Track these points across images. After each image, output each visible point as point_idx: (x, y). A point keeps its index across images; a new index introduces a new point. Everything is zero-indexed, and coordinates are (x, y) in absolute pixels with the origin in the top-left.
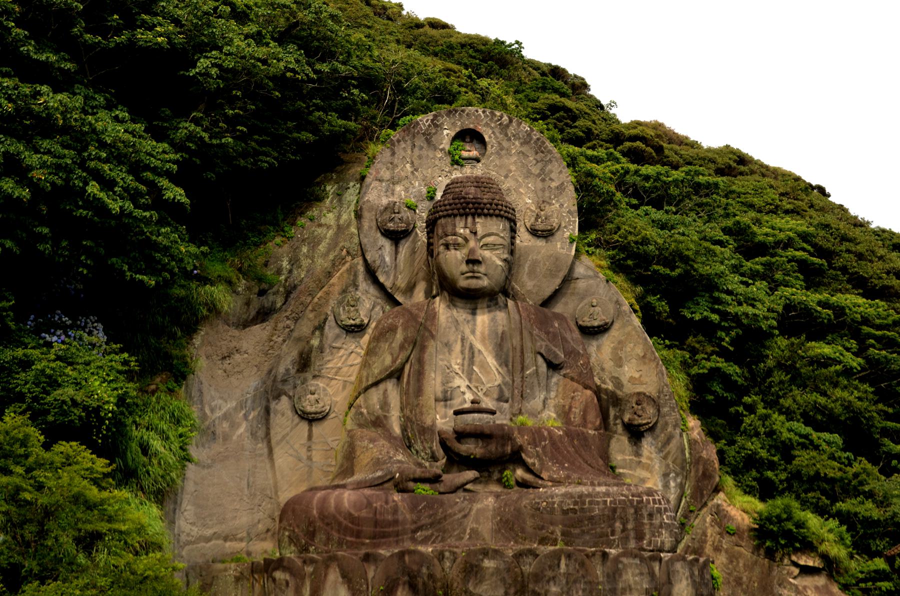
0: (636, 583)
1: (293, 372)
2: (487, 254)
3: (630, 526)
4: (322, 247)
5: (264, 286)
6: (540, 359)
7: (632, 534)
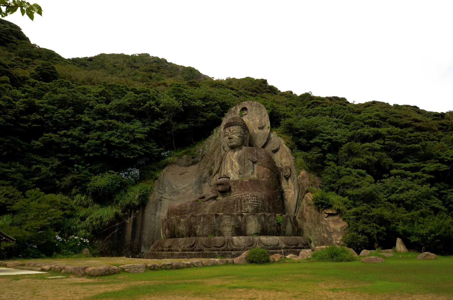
0: (228, 223)
1: (208, 176)
2: (234, 135)
3: (239, 205)
4: (211, 145)
5: (194, 156)
6: (250, 161)
7: (239, 208)
